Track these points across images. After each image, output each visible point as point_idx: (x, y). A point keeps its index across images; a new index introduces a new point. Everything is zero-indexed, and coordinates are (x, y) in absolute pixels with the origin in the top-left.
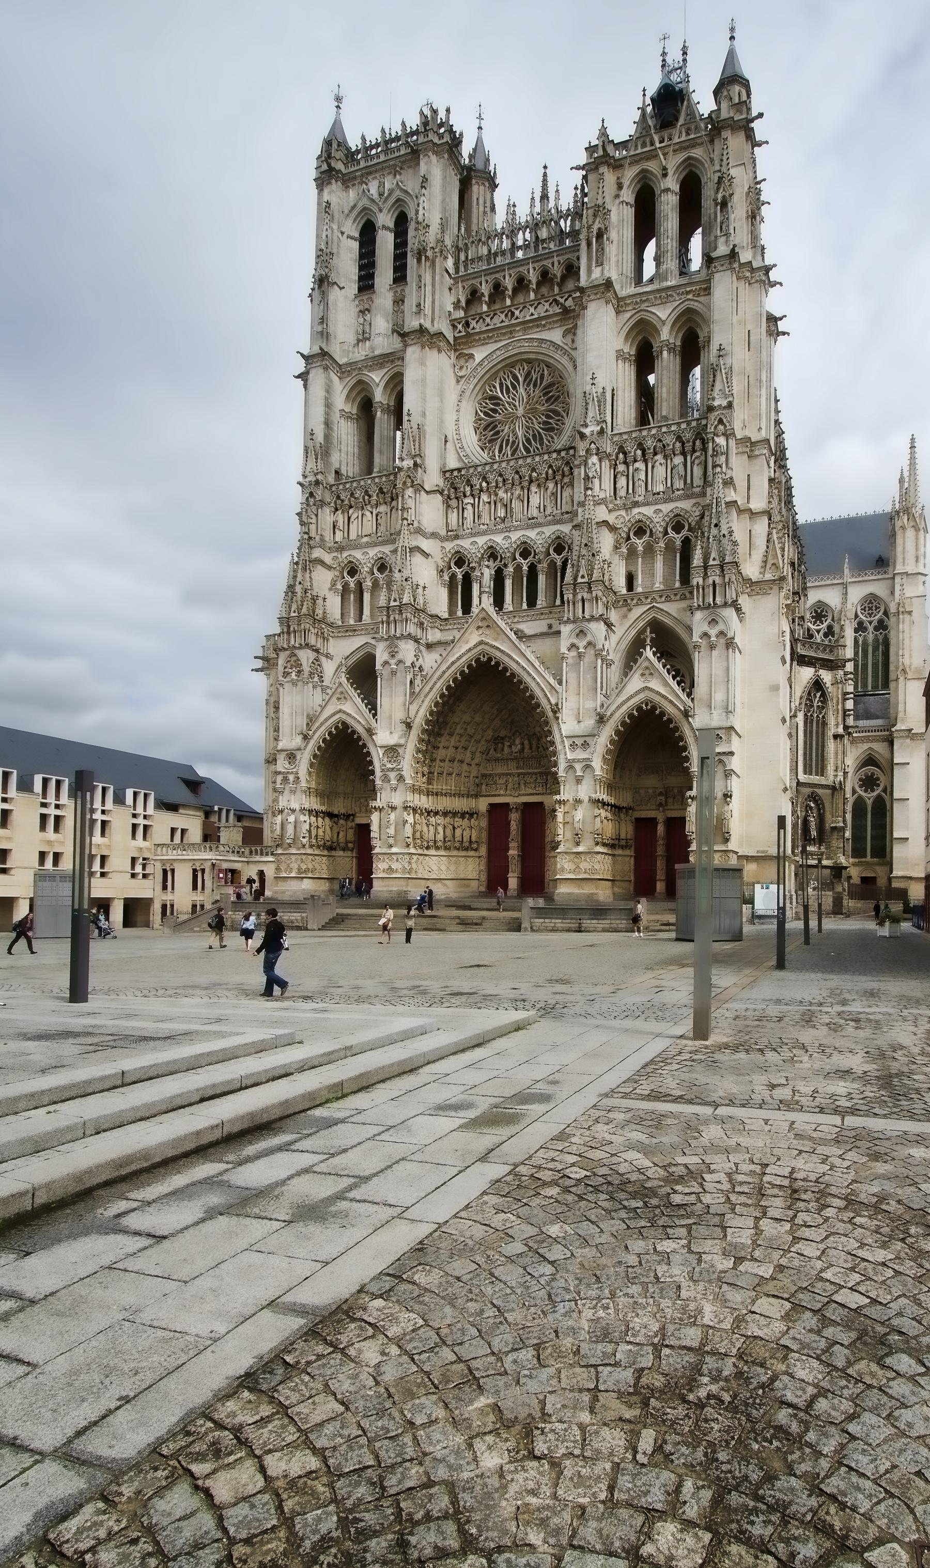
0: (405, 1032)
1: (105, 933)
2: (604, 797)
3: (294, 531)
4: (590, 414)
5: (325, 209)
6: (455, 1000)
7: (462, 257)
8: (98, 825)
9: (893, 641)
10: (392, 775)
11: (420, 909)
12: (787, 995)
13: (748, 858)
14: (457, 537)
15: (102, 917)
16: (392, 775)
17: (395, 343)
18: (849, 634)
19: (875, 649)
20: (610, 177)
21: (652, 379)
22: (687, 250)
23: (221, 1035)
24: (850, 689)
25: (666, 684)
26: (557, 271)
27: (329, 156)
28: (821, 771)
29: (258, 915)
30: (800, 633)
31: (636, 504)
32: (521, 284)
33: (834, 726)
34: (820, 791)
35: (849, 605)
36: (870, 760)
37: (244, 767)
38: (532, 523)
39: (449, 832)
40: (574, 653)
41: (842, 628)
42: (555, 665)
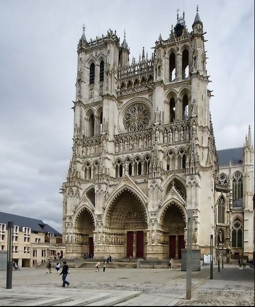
0: (103, 297)
1: (16, 269)
2: (161, 229)
3: (71, 152)
4: (157, 119)
5: (80, 60)
6: (118, 288)
7: (120, 74)
8: (15, 238)
9: (244, 184)
10: (99, 223)
11: (107, 262)
12: (213, 287)
13: (202, 247)
14: (118, 154)
15: (16, 264)
16: (99, 223)
17: (101, 98)
18: (231, 182)
19: (239, 187)
20: (162, 51)
21: (174, 109)
22: (185, 72)
23: (50, 298)
24: (232, 198)
25: (178, 197)
26: (147, 78)
27: (81, 45)
28: (223, 222)
29: (61, 264)
30: (217, 182)
31: (170, 145)
32: (137, 82)
33: (227, 209)
34: (223, 228)
35: (231, 174)
36: (237, 219)
37: (57, 221)
38: (140, 150)
39: (116, 240)
40: (152, 188)
41: (229, 180)
42: (146, 191)
